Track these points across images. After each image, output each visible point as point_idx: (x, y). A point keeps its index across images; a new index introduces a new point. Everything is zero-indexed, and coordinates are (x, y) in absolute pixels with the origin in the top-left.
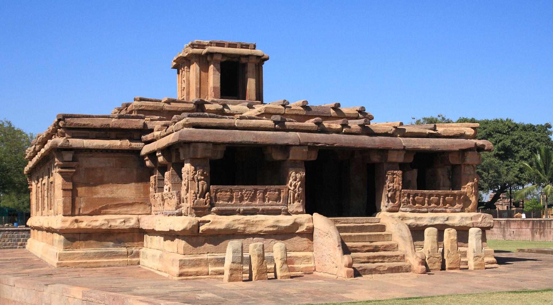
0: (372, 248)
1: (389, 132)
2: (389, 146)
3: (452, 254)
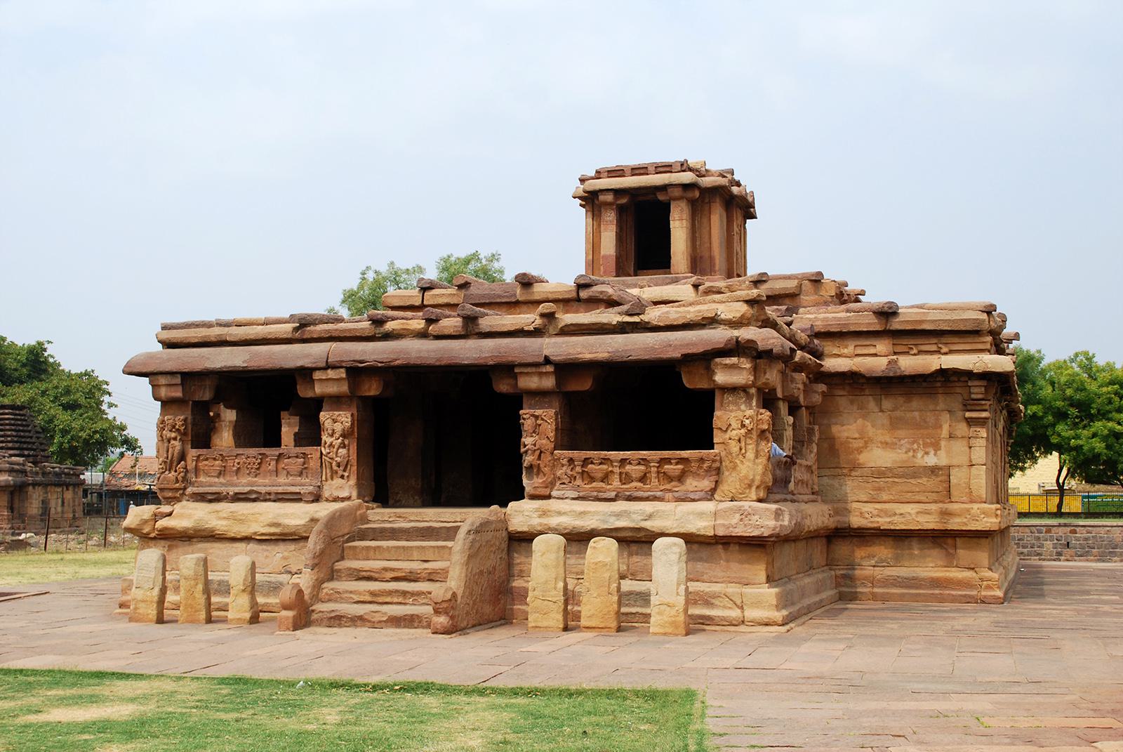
0: (404, 574)
1: (526, 328)
2: (510, 359)
3: (595, 595)
